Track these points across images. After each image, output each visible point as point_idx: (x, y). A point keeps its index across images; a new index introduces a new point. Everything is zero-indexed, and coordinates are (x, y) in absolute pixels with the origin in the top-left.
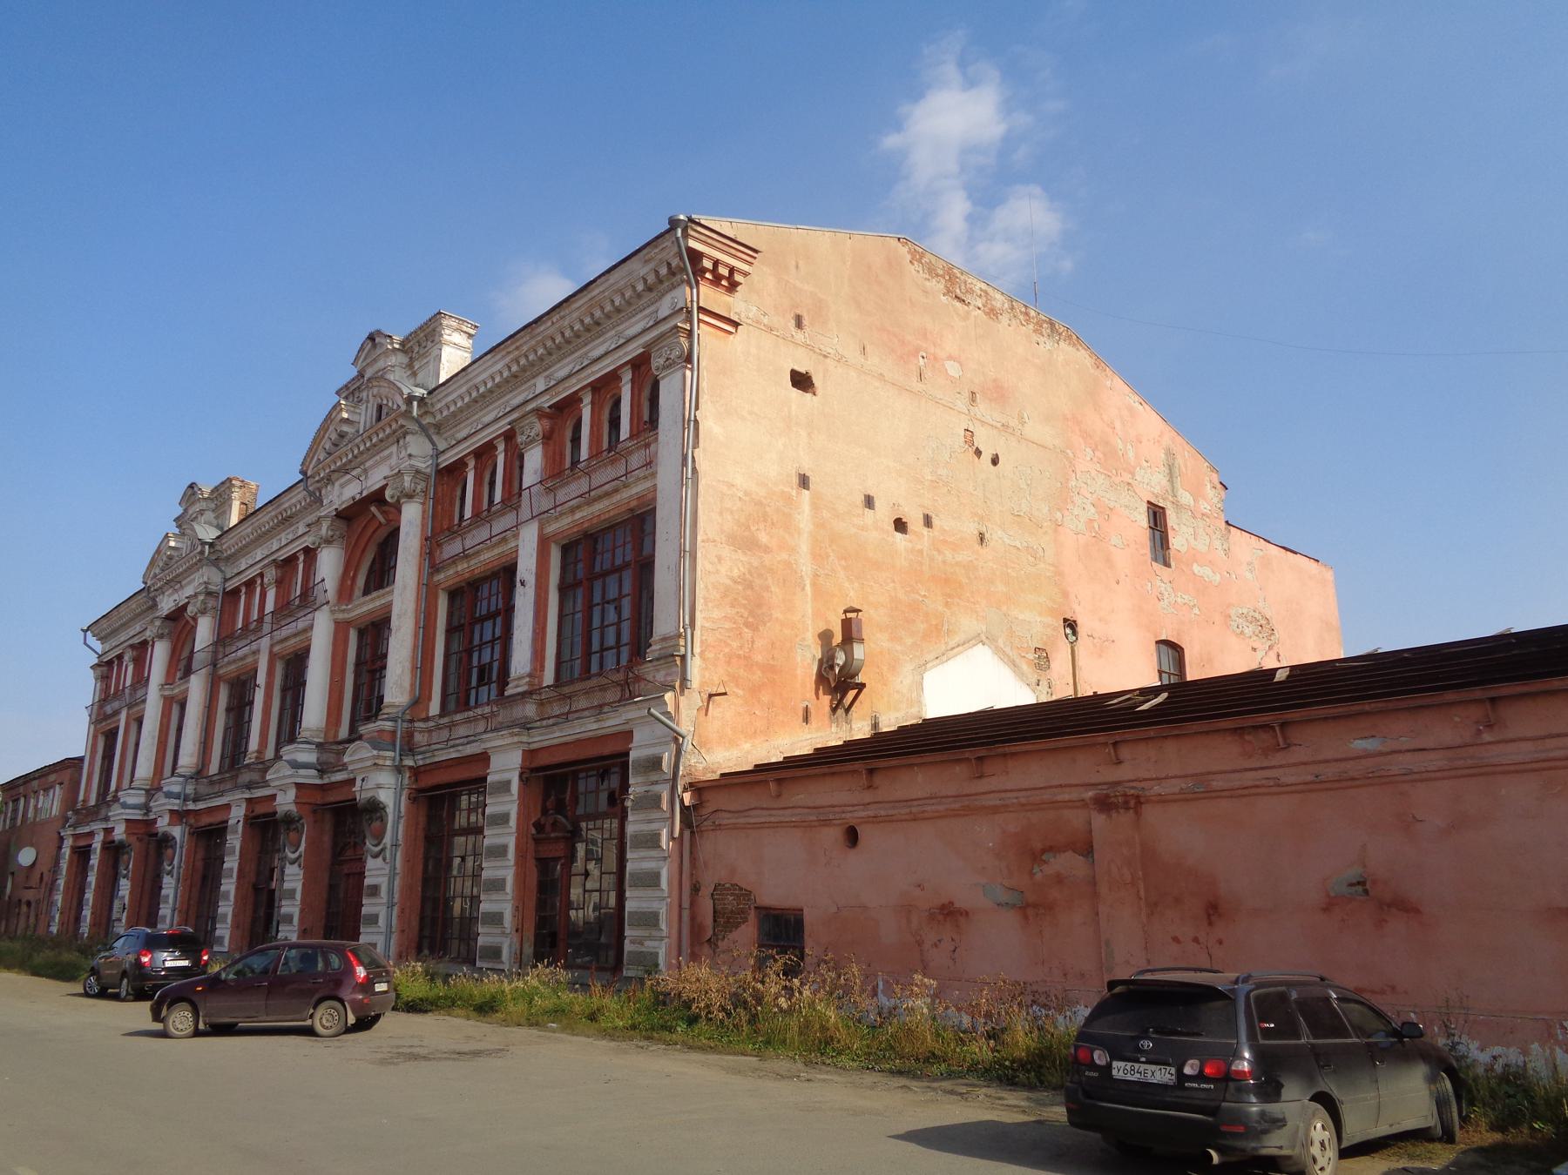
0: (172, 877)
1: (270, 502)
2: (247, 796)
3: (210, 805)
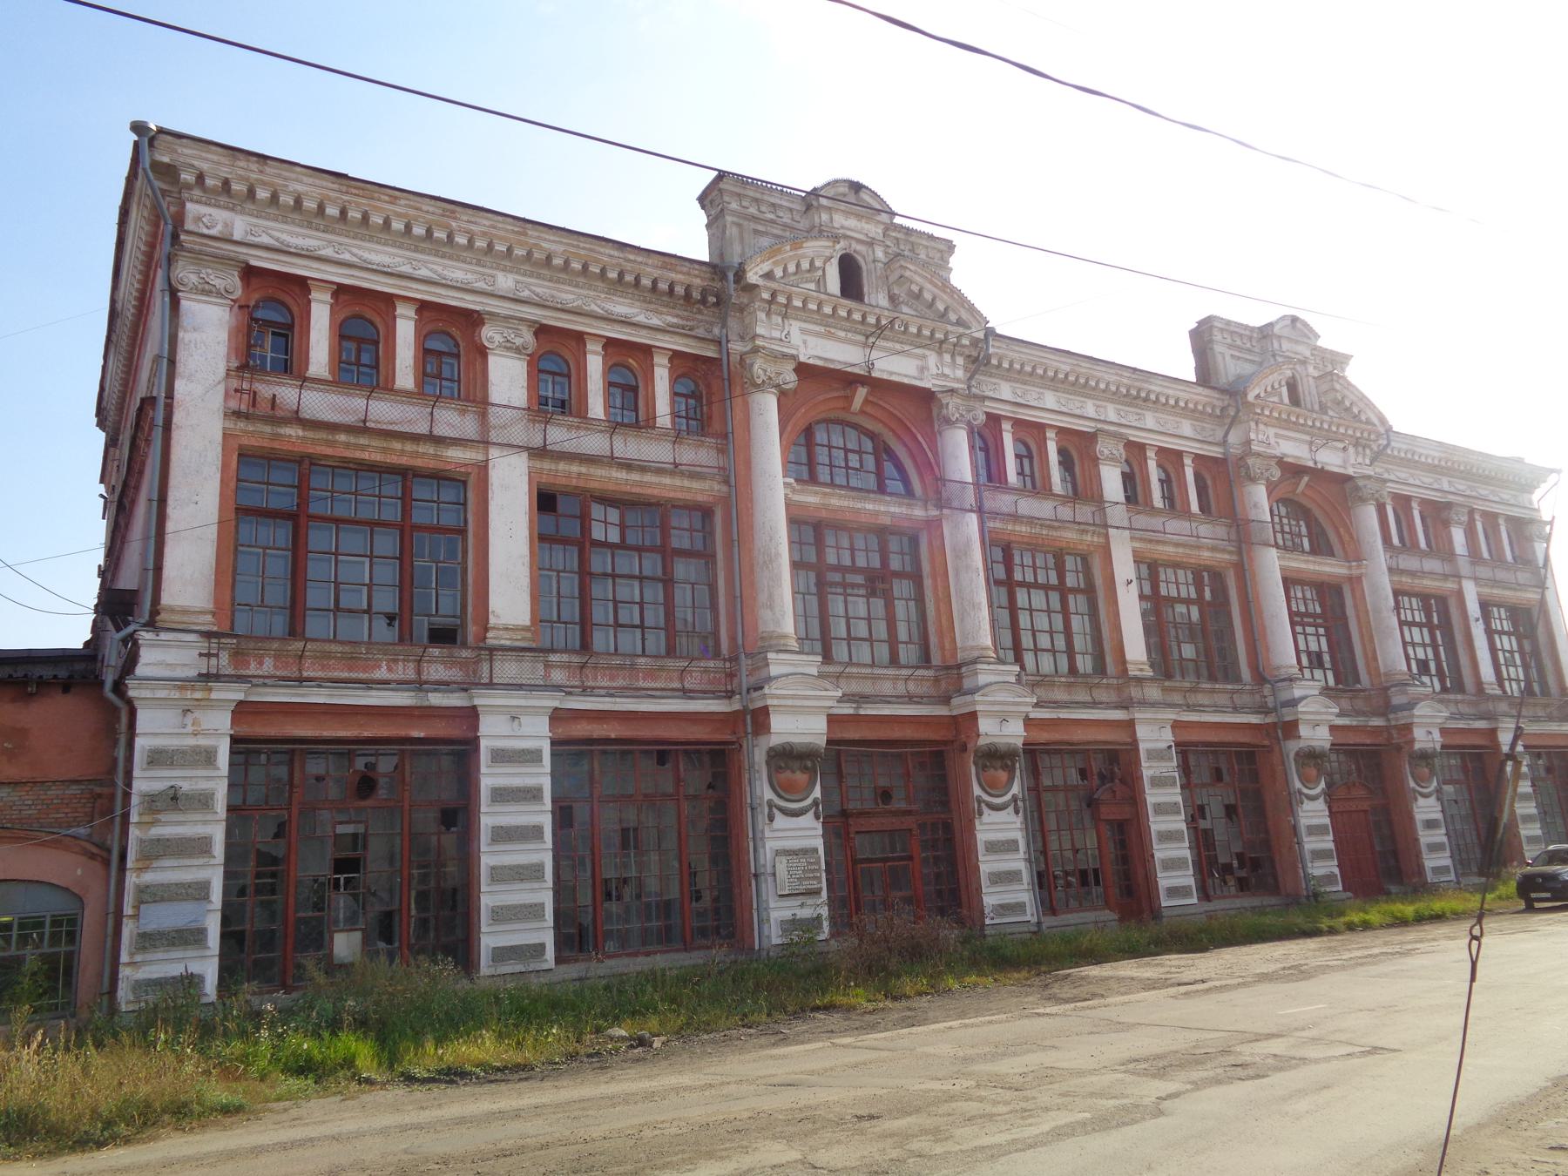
0: (1017, 812)
1: (1135, 370)
2: (1174, 717)
3: (1062, 716)
